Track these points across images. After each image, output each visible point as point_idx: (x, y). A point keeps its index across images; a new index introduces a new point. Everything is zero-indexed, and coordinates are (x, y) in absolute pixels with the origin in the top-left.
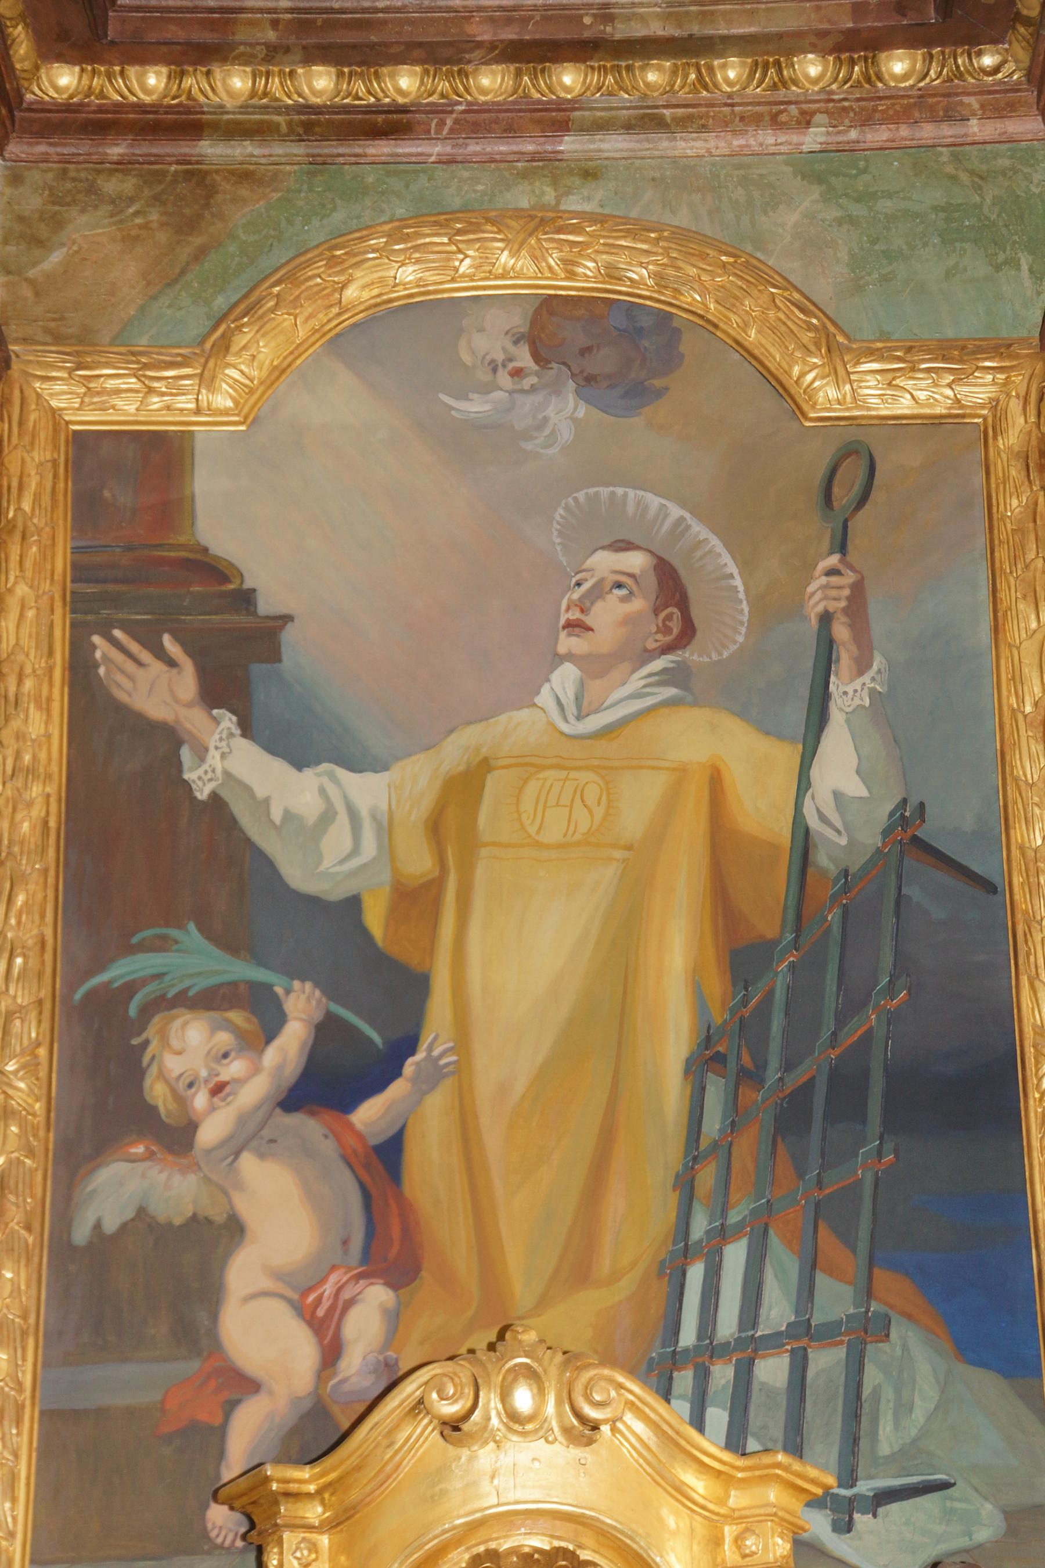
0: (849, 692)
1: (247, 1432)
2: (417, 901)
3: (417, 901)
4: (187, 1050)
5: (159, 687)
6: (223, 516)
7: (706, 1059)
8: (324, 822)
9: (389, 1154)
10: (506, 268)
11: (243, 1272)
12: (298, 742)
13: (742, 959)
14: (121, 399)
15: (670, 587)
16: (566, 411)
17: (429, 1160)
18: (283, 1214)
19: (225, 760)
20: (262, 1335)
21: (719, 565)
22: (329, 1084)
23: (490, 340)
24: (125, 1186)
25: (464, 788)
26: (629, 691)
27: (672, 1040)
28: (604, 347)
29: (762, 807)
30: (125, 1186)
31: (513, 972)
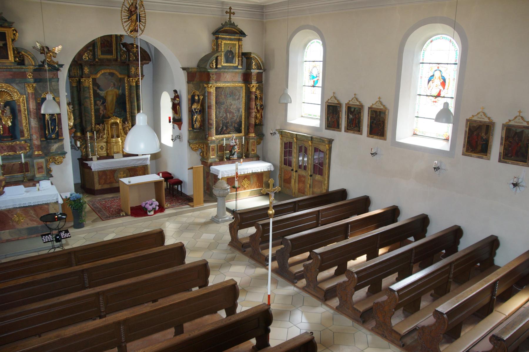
0: (121, 88)
1: (101, 115)
2: (106, 96)
3: (106, 96)
4: (98, 102)
5: (96, 88)
6: (98, 81)
7: (116, 102)
8: (102, 93)
9: (105, 106)
10: (108, 71)
11: (101, 110)
12: (101, 90)
13: (117, 98)
14: (94, 77)
15: (114, 84)
16: (110, 77)
17: (107, 106)
18: (102, 108)
19: (98, 91)
20: (101, 112)
21: (116, 83)
22: (103, 103)
23: (107, 74)
24: (96, 107)
25: (107, 92)
26: (113, 88)
27: (115, 101)
28: (112, 74)
29: (118, 93)
30: (96, 107)
31: (109, 99)
